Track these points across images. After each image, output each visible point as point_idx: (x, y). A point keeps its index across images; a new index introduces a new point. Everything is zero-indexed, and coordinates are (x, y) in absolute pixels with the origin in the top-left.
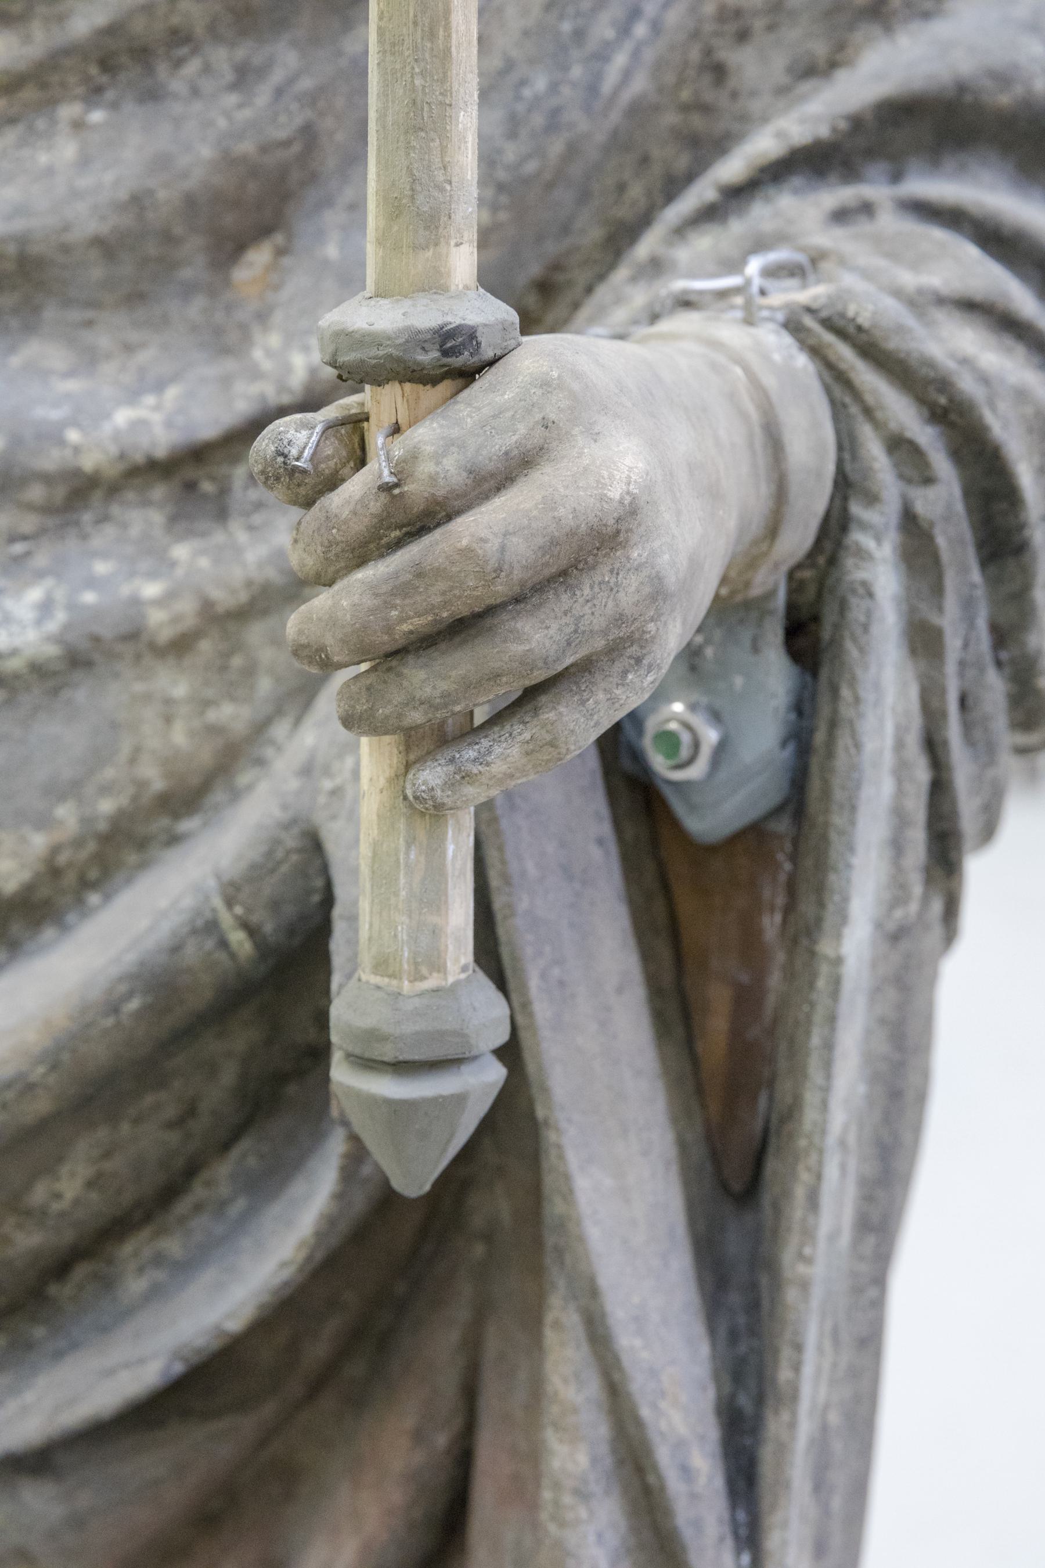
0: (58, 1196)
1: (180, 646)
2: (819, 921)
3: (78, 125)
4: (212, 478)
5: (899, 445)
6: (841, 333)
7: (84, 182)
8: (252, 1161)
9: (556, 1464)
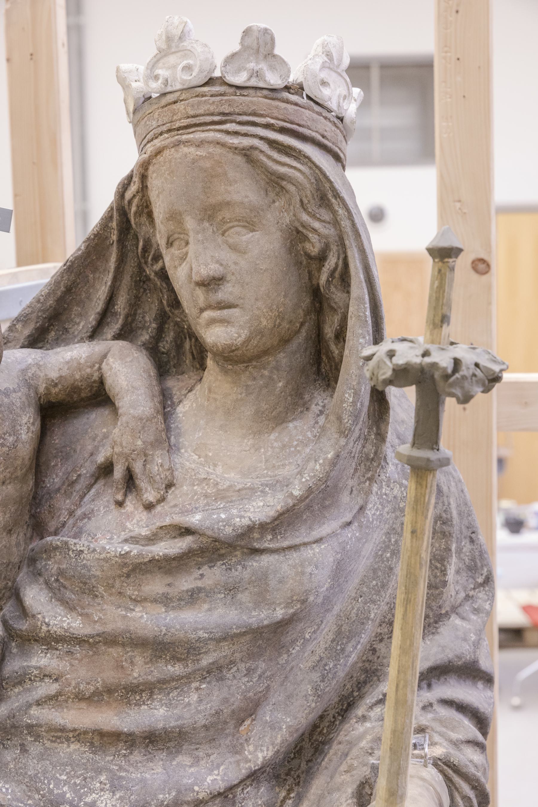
3: (197, 689)
4: (232, 794)
6: (449, 766)
7: (202, 708)
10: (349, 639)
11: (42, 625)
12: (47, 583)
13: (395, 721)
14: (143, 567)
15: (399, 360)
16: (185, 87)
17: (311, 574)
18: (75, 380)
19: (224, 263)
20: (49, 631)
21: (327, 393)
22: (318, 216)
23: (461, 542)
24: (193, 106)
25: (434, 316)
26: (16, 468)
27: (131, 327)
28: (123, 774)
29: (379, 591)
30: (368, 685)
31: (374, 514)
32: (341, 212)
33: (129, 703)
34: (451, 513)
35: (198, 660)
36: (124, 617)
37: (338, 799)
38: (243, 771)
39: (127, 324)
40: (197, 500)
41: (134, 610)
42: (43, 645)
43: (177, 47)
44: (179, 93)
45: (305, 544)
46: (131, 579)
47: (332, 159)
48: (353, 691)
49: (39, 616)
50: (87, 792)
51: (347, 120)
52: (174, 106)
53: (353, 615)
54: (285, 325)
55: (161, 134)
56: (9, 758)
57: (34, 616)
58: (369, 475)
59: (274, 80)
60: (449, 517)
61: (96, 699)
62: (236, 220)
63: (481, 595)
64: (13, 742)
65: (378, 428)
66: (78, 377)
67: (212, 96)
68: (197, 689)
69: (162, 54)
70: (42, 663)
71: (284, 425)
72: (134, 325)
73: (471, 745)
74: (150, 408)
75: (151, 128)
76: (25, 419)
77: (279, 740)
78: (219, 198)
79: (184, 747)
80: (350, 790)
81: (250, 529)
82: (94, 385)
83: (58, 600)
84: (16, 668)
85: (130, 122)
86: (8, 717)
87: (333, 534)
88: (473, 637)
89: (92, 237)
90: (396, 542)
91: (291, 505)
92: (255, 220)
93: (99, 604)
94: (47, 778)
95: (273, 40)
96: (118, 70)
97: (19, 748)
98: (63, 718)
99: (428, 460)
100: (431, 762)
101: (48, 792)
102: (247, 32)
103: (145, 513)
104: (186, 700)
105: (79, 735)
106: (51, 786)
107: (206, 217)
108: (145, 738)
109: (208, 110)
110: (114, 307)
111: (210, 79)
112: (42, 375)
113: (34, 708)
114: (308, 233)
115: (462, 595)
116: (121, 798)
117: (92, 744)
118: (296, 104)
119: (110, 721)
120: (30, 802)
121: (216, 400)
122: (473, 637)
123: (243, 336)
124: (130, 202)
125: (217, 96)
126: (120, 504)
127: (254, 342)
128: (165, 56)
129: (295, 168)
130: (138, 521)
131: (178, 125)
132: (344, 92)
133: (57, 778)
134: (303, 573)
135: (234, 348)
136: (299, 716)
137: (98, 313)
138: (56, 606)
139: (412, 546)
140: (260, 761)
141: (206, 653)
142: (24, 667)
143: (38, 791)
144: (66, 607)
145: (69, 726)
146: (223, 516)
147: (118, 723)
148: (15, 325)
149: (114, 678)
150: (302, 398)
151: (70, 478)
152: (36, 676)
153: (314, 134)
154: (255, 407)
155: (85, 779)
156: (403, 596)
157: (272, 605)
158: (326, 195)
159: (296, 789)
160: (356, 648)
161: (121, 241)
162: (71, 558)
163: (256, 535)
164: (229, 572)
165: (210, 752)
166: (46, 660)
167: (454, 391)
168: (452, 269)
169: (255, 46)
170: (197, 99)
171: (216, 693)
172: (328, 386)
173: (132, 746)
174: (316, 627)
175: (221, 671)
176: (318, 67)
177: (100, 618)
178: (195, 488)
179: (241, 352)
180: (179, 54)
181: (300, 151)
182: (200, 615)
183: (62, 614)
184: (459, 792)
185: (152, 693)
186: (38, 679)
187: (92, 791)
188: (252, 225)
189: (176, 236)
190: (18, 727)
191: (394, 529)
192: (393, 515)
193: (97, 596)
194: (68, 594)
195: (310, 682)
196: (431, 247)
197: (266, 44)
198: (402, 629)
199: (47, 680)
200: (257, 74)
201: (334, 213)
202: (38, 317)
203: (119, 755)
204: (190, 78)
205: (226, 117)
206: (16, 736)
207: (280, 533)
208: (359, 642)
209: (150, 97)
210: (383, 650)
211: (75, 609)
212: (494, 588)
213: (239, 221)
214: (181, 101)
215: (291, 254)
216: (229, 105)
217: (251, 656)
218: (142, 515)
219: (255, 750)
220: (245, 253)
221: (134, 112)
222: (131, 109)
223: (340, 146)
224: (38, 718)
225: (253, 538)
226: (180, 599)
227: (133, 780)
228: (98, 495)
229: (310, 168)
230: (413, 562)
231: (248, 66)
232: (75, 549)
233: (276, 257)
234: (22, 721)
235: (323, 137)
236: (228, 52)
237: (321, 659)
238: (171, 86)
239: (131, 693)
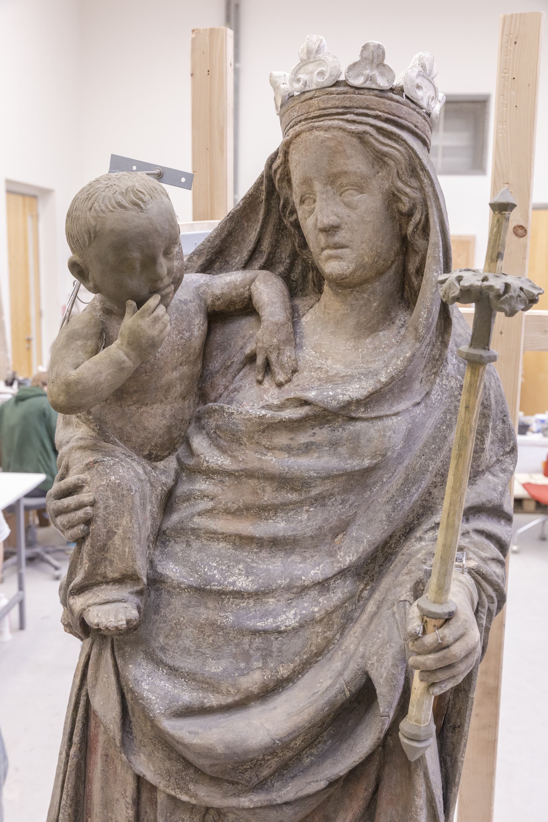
0: (296, 744)
1: (321, 620)
2: (469, 690)
3: (307, 511)
5: (489, 597)
8: (331, 731)
9: (416, 803)
10: (414, 484)
12: (208, 434)
13: (446, 539)
14: (275, 426)
15: (465, 283)
16: (319, 87)
17: (390, 437)
18: (232, 296)
19: (340, 216)
20: (208, 466)
21: (407, 312)
22: (409, 183)
23: (496, 422)
24: (324, 101)
25: (492, 253)
26: (190, 354)
27: (272, 262)
28: (254, 565)
29: (437, 452)
30: (425, 517)
31: (436, 398)
32: (426, 181)
33: (260, 518)
34: (490, 401)
35: (309, 491)
36: (260, 459)
37: (400, 592)
38: (336, 569)
39: (269, 260)
40: (313, 382)
41: (266, 455)
43: (314, 58)
44: (314, 92)
45: (387, 416)
46: (266, 434)
47: (421, 143)
48: (414, 520)
50: (229, 575)
51: (433, 116)
52: (310, 102)
53: (417, 468)
54: (381, 262)
55: (300, 122)
56: (178, 550)
57: (198, 456)
58: (435, 371)
59: (383, 83)
60: (489, 403)
61: (238, 513)
62: (351, 185)
63: (507, 460)
64: (181, 539)
65: (443, 338)
66: (234, 294)
67: (338, 94)
68: (307, 511)
69: (304, 63)
70: (203, 487)
71: (376, 333)
72: (273, 260)
73: (495, 561)
74: (284, 317)
75: (293, 117)
76: (197, 321)
77: (361, 549)
78: (339, 169)
79: (296, 550)
80: (409, 586)
81: (349, 403)
82: (245, 300)
83: (215, 446)
84: (185, 490)
85: (278, 115)
86: (179, 522)
87: (407, 410)
88: (500, 489)
89: (248, 196)
90: (450, 419)
91: (379, 388)
92: (364, 185)
93: (243, 450)
94: (203, 564)
95: (384, 53)
96: (271, 76)
98: (215, 525)
99: (481, 356)
100: (467, 570)
101: (203, 573)
102: (365, 47)
103: (277, 389)
104: (299, 518)
105: (226, 537)
106: (206, 570)
107: (329, 182)
108: (270, 542)
109: (335, 104)
110: (261, 246)
111: (337, 82)
112: (210, 291)
113: (196, 517)
114: (401, 196)
115: (494, 459)
116: (252, 581)
117: (234, 544)
118: (398, 102)
119: (247, 529)
120: (191, 579)
121: (329, 313)
122: (500, 489)
123: (351, 268)
124: (276, 171)
125: (341, 94)
126: (260, 382)
127: (359, 273)
128: (306, 64)
129: (394, 148)
130: (272, 395)
131: (312, 115)
132: (433, 95)
133: (210, 565)
134: (384, 436)
135: (344, 277)
136: (376, 534)
137: (250, 251)
138: (213, 450)
139: (465, 417)
140: (347, 563)
141: (314, 487)
142: (190, 490)
143: (197, 572)
144: (220, 451)
145: (219, 530)
146: (331, 393)
147: (253, 531)
148: (192, 257)
149: (251, 500)
150: (390, 315)
151: (226, 364)
153: (409, 124)
154: (356, 320)
155: (229, 566)
156: (456, 452)
157: (362, 456)
158: (415, 169)
159: (371, 584)
160: (418, 490)
161: (268, 200)
162: (225, 417)
163: (353, 408)
164: (333, 432)
165: (314, 554)
166: (205, 485)
167: (503, 306)
168: (508, 219)
169: (371, 57)
170: (327, 96)
171: (320, 515)
172: (409, 307)
173: (261, 546)
174: (391, 474)
175: (324, 500)
176: (415, 74)
177: (243, 459)
178: (312, 374)
179: (348, 280)
180: (315, 63)
181: (399, 136)
182: (311, 461)
183: (218, 455)
184: (485, 593)
185: (276, 512)
187: (233, 575)
188: (362, 189)
189: (307, 196)
190: (185, 529)
191: (449, 410)
192: (450, 400)
193: (241, 444)
194: (222, 442)
195: (384, 513)
196: (493, 202)
197: (379, 56)
198: (454, 475)
200: (371, 78)
201: (421, 181)
202: (208, 252)
203: (252, 552)
204: (323, 80)
205: (347, 110)
206: (184, 535)
207: (370, 407)
208: (420, 486)
209: (293, 96)
210: (436, 494)
211: (226, 452)
212: (517, 456)
213: (352, 185)
214: (316, 97)
215: (388, 211)
216: (350, 101)
217: (345, 491)
218: (275, 391)
219: (345, 555)
220: (355, 209)
221: (281, 107)
222: (279, 104)
223: (427, 134)
224: (199, 524)
225: (351, 410)
226: (299, 449)
227: (261, 569)
228: (245, 376)
229: (406, 148)
230: (465, 428)
231: (364, 72)
233: (378, 213)
235: (416, 126)
236: (351, 62)
237: (393, 496)
238: (309, 86)
239: (263, 511)
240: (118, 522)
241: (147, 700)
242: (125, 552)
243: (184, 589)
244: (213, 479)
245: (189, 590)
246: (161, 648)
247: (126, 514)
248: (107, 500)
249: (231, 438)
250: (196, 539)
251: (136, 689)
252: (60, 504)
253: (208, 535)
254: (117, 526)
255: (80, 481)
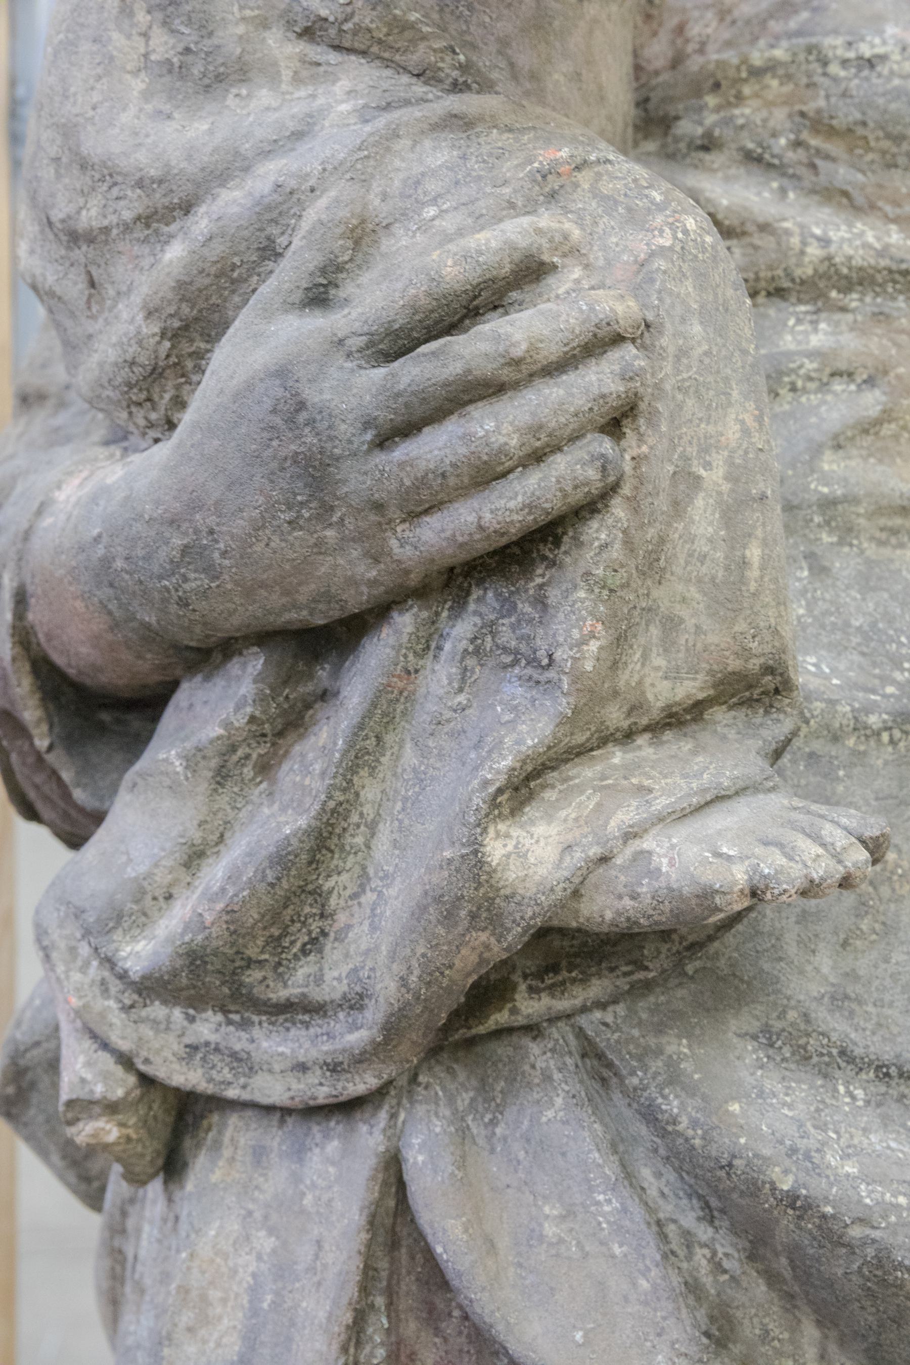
11: (804, 243)
20: (829, 258)
42: (800, 301)
49: (787, 225)
57: (764, 228)
83: (813, 191)
97: (804, 564)
113: (828, 455)
152: (810, 379)
162: (835, 79)
166: (821, 336)
186: (812, 386)
190: (798, 507)
194: (843, 174)
199: (838, 386)
232: (851, 55)
234: (806, 489)
240: (711, 429)
241: (885, 1217)
242: (744, 563)
243: (878, 734)
244: (844, 309)
245: (897, 734)
246: (833, 998)
247: (735, 394)
248: (683, 320)
249: (884, 153)
250: (841, 542)
251: (817, 1188)
252: (484, 347)
253: (882, 521)
254: (705, 450)
255: (544, 242)
